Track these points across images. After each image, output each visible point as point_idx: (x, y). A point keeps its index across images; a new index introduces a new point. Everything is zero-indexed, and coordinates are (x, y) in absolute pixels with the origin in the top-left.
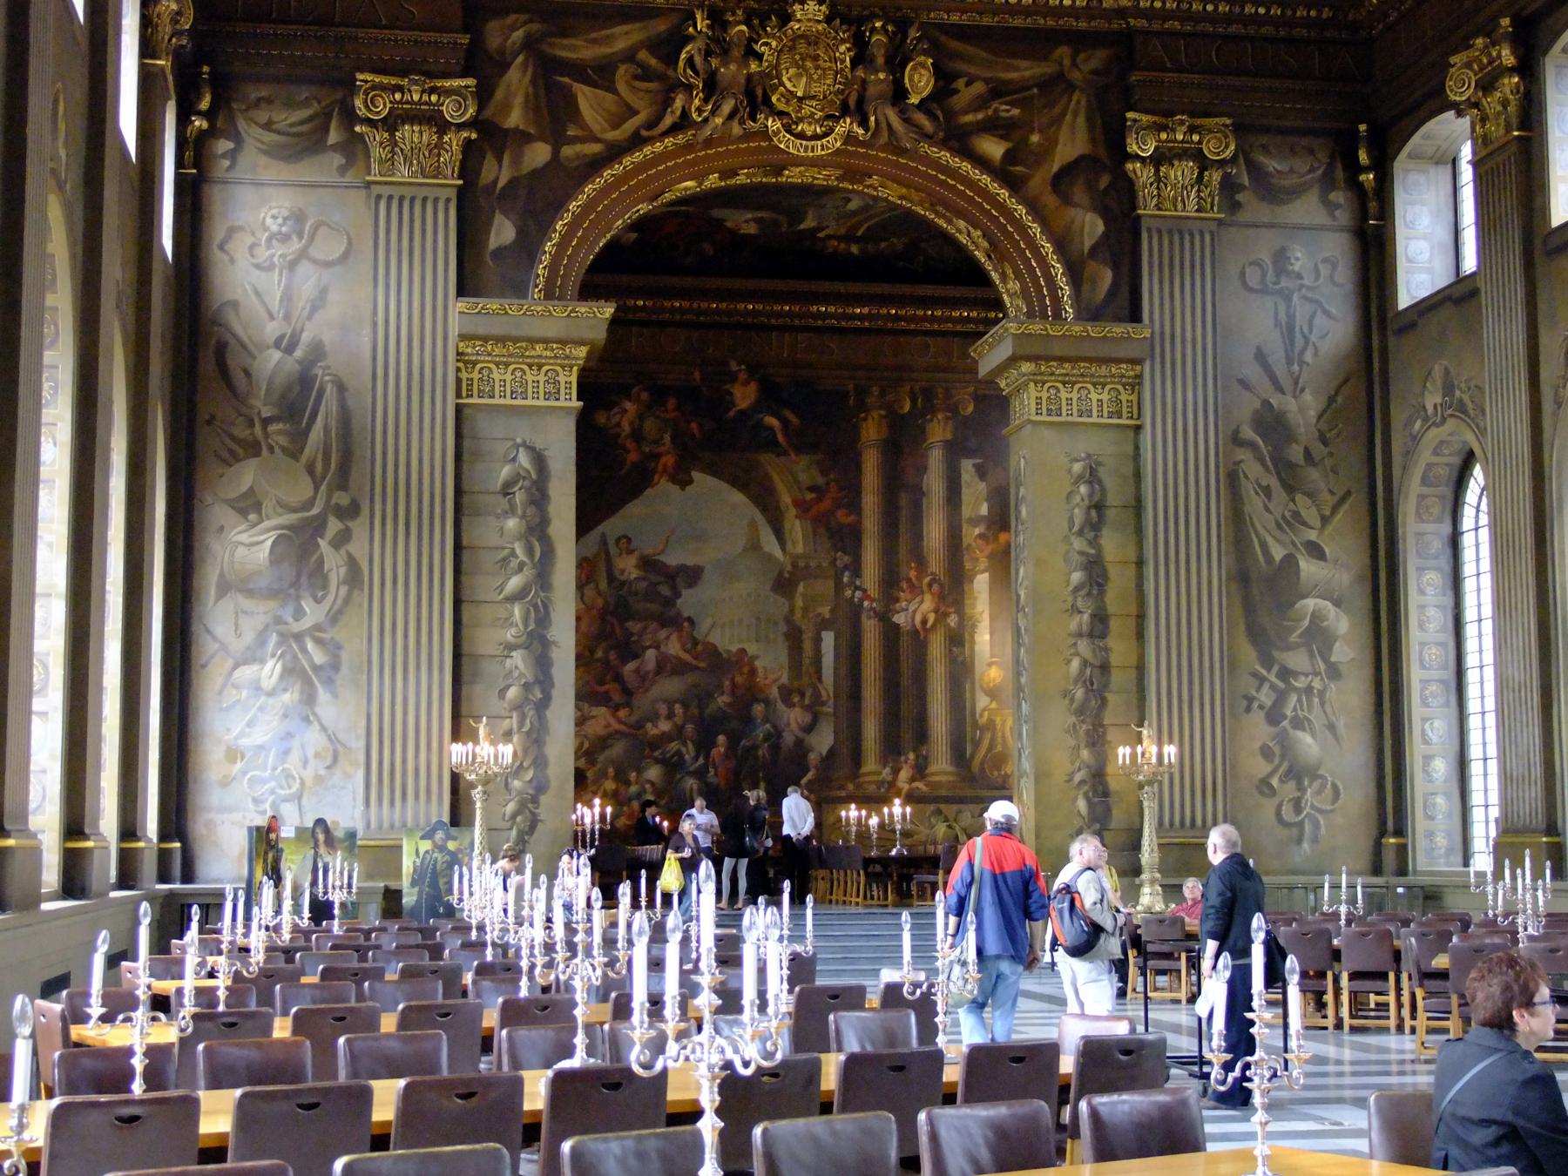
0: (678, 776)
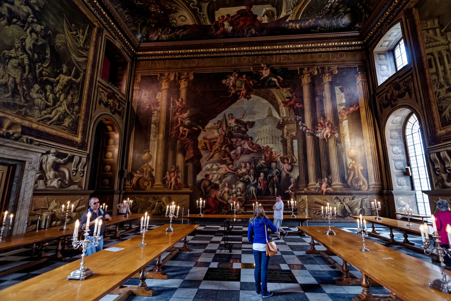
0: (248, 186)
